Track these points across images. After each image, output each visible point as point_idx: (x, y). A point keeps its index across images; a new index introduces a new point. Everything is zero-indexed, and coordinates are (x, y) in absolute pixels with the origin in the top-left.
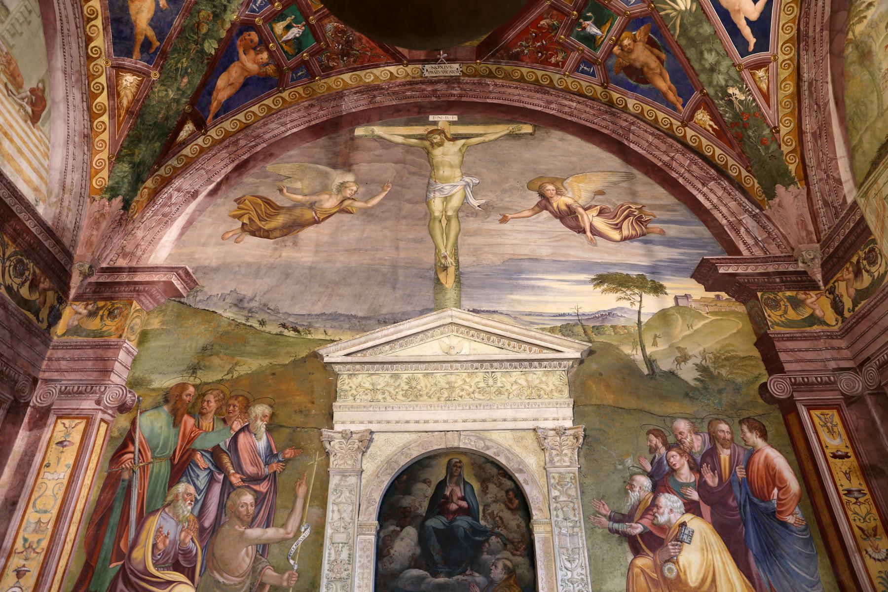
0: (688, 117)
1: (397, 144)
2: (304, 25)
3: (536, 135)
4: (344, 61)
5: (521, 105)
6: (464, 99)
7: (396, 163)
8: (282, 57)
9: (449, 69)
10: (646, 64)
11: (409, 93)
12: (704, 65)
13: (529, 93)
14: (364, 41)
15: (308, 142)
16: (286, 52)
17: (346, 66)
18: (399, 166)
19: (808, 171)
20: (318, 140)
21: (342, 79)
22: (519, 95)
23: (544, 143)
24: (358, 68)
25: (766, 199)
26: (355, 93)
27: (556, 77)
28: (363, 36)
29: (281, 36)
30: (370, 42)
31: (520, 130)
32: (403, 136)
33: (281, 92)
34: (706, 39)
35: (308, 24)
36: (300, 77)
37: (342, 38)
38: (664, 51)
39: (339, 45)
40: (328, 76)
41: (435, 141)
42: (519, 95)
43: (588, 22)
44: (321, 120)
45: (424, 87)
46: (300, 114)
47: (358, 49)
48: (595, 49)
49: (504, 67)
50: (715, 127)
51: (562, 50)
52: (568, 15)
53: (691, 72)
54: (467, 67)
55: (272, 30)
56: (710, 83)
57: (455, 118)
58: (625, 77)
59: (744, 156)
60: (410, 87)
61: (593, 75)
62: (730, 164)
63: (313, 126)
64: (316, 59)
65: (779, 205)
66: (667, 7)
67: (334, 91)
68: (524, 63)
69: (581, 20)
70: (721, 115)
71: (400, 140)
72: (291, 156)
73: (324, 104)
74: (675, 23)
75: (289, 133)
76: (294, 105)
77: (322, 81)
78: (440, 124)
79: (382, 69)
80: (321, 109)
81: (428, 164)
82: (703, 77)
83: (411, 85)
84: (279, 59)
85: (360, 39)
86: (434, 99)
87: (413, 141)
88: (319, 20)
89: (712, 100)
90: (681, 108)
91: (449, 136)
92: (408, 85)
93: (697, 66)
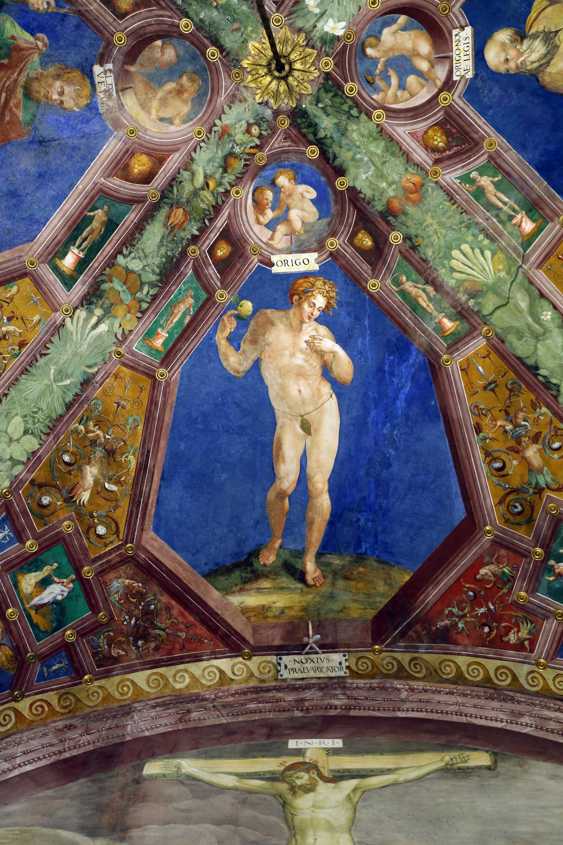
1: (222, 790)
2: (72, 581)
3: (499, 769)
4: (138, 647)
5: (464, 719)
6: (353, 713)
7: (219, 823)
8: (28, 634)
9: (325, 664)
11: (252, 706)
13: (476, 701)
14: (175, 612)
15: (49, 789)
16: (34, 626)
17: (141, 657)
18: (224, 830)
20: (70, 784)
21: (132, 682)
22: (457, 704)
23: (519, 784)
24: (163, 660)
26: (154, 707)
27: (522, 670)
28: (173, 603)
29: (31, 596)
30: (186, 613)
31: (466, 761)
32: (236, 775)
33: (15, 700)
35: (80, 579)
36: (56, 674)
37: (136, 605)
39: (130, 619)
40: (107, 674)
41: (299, 782)
42: (457, 704)
44: (82, 751)
45: (280, 695)
46: (45, 741)
47: (163, 626)
49: (426, 657)
51: (526, 618)
52: (526, 554)
54: (359, 659)
55: (16, 584)
57: (338, 743)
60: (254, 696)
63: (66, 761)
64: (88, 642)
67: (116, 705)
68: (460, 648)
69: (552, 562)
71: (230, 781)
72: (8, 815)
73: (92, 725)
75: (17, 772)
76: (39, 726)
77: (96, 683)
78: (308, 754)
79: (204, 664)
80: (87, 732)
81: (284, 826)
83: (257, 692)
84: (21, 637)
85: (168, 608)
86: (298, 714)
87: (256, 783)
88: (100, 573)
91: (326, 774)
92: (252, 692)
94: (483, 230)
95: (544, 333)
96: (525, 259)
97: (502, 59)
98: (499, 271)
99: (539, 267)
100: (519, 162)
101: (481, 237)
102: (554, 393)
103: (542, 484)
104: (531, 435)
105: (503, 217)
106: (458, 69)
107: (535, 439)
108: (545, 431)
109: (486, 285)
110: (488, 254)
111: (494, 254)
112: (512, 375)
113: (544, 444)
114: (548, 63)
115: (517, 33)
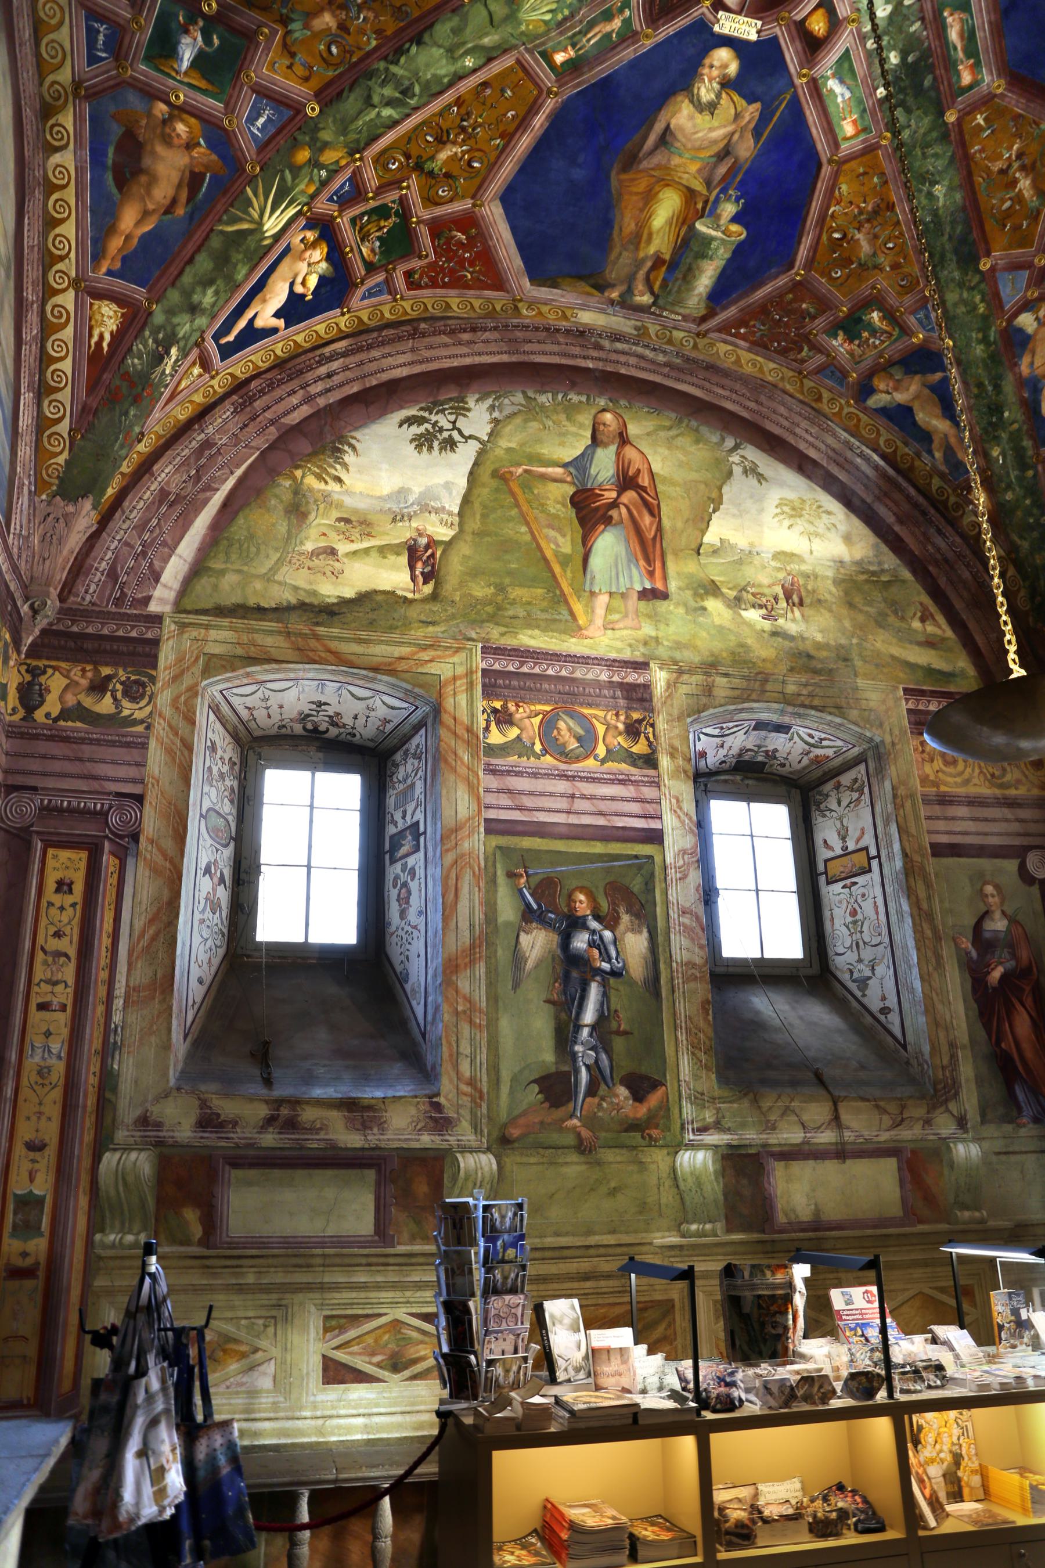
0: (95, 288)
10: (153, 179)
12: (193, 291)
19: (117, 515)
25: (55, 488)
34: (229, 278)
38: (189, 209)
43: (200, 38)
48: (148, 59)
50: (105, 345)
53: (173, 270)
56: (170, 312)
58: (114, 138)
59: (91, 418)
61: (93, 59)
62: (59, 396)
65: (66, 516)
66: (262, 198)
70: (130, 349)
74: (240, 220)
82: (174, 296)
89: (145, 324)
90: (104, 270)
93: (187, 279)
94: (572, 15)
95: (453, 58)
96: (529, 51)
97: (716, 63)
98: (527, 26)
99: (518, 61)
100: (620, 60)
101: (566, 12)
102: (390, 57)
103: (293, 26)
104: (348, 23)
105: (576, 39)
106: (727, 18)
107: (343, 27)
108: (350, 40)
109: (518, 10)
110: (548, 17)
111: (545, 22)
112: (416, 14)
113: (336, 35)
114: (692, 102)
115: (729, 81)
